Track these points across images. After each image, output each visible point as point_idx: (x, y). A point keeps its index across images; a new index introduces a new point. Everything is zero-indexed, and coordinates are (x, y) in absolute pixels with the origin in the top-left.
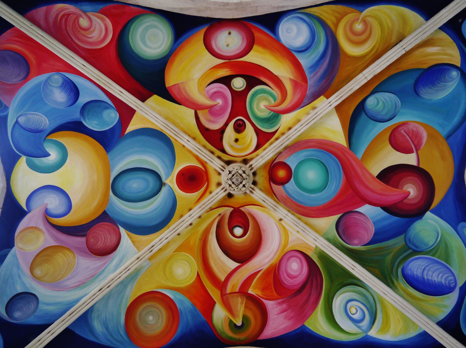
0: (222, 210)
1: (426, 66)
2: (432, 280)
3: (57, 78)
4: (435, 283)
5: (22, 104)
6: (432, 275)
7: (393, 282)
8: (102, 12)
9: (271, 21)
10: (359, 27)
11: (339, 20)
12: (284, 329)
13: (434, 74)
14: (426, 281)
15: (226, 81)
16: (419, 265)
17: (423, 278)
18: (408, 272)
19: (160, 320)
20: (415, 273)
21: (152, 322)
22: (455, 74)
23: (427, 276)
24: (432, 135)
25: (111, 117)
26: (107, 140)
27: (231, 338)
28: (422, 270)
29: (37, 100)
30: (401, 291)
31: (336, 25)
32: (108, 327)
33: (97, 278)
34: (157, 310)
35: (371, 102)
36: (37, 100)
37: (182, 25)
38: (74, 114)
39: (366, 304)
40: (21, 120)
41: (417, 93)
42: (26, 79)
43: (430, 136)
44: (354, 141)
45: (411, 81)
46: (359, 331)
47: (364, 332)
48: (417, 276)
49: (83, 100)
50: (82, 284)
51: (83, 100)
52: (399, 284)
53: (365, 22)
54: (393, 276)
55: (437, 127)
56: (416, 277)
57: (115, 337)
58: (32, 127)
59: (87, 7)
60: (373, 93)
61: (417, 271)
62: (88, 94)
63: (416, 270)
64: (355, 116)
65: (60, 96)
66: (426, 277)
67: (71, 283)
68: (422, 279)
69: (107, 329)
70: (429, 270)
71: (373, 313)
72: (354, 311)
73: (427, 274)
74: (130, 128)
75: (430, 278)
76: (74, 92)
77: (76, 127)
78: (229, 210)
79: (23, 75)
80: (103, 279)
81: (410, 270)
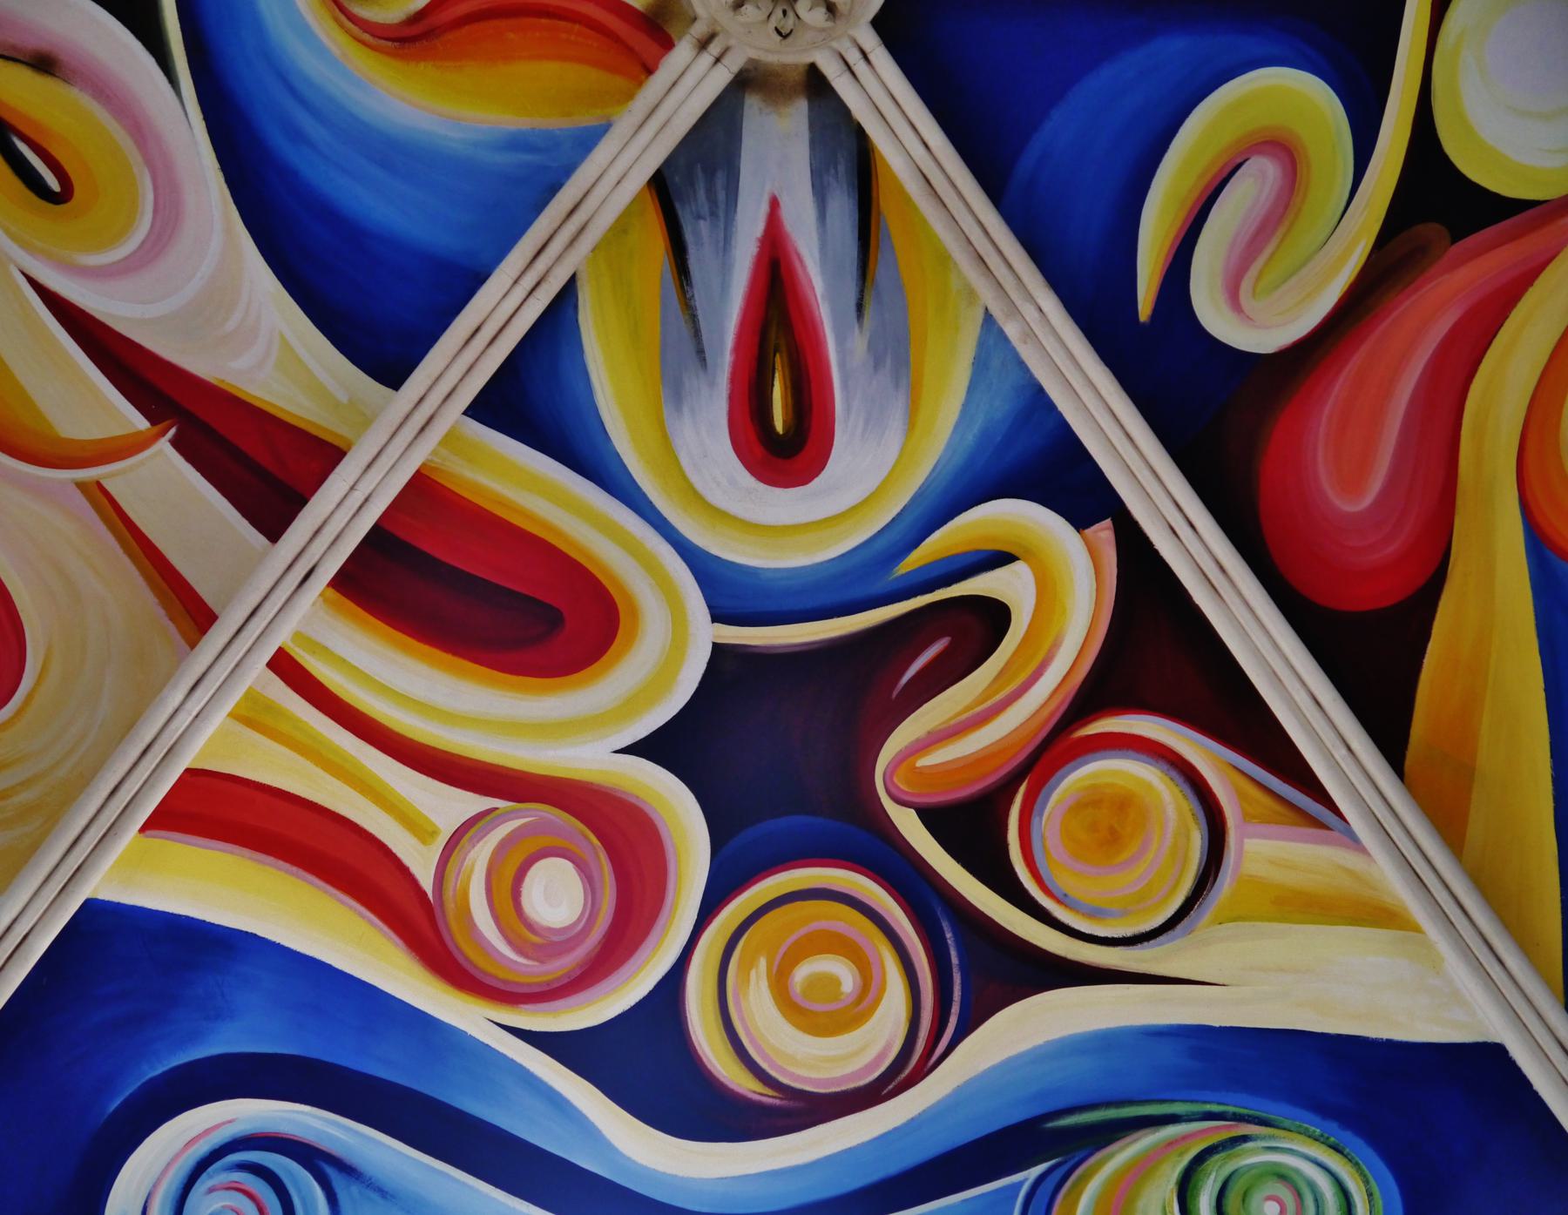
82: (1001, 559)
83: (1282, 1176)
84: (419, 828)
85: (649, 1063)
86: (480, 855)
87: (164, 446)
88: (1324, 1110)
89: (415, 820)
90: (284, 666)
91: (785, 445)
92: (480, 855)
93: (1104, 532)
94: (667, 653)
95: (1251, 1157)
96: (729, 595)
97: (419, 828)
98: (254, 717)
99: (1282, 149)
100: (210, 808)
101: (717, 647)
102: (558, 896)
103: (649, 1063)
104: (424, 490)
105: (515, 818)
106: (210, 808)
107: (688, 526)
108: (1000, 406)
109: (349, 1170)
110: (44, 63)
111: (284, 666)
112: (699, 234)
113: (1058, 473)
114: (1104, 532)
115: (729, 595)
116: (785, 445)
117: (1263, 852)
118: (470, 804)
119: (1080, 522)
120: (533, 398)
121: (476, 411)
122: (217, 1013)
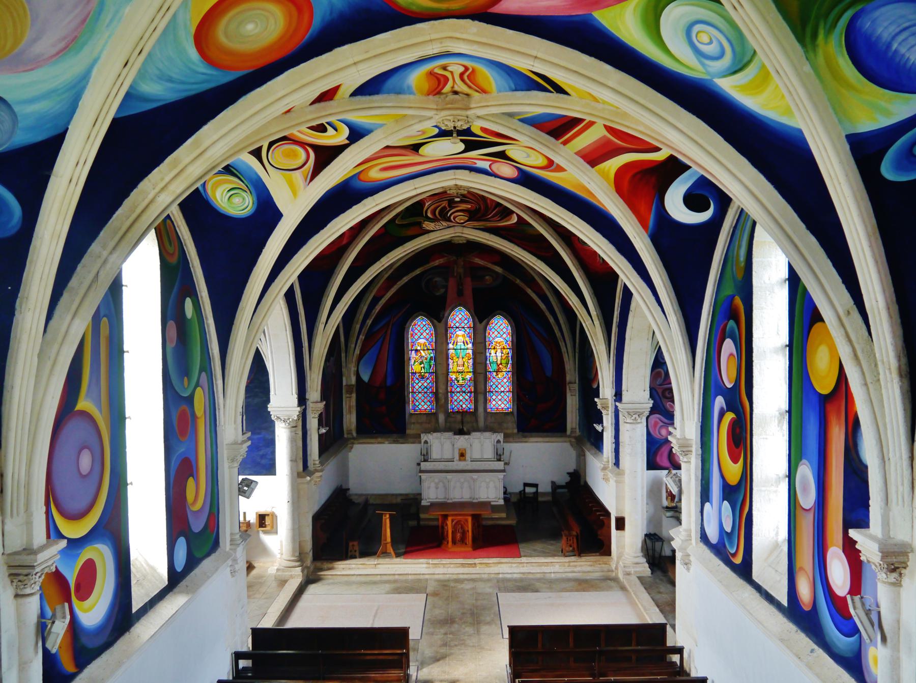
2: (903, 55)
4: (905, 63)
6: (912, 46)
7: (815, 36)
12: (548, 8)
14: (890, 54)
16: (902, 17)
17: (889, 46)
18: (866, 24)
19: (272, 21)
20: (879, 30)
21: (257, 31)
23: (900, 44)
27: (433, 9)
28: (898, 30)
30: (821, 59)
32: (171, 77)
33: (97, 19)
34: (259, 12)
39: (734, 42)
46: (699, 67)
47: (708, 73)
48: (879, 37)
50: (71, 44)
52: (826, 42)
54: (825, 24)
56: (873, 39)
57: (192, 80)
61: (886, 28)
63: (885, 24)
66: (895, 46)
67: (45, 45)
68: (884, 47)
69: (170, 80)
70: (913, 34)
71: (740, 61)
72: (705, 38)
73: (904, 40)
75: (903, 50)
80: (111, 21)
81: (874, 21)
82: (336, 130)
83: (244, 199)
88: (258, 199)
93: (347, 142)
95: (244, 194)
108: (367, 127)
113: (356, 134)
114: (347, 142)
117: (298, 176)
119: (347, 139)
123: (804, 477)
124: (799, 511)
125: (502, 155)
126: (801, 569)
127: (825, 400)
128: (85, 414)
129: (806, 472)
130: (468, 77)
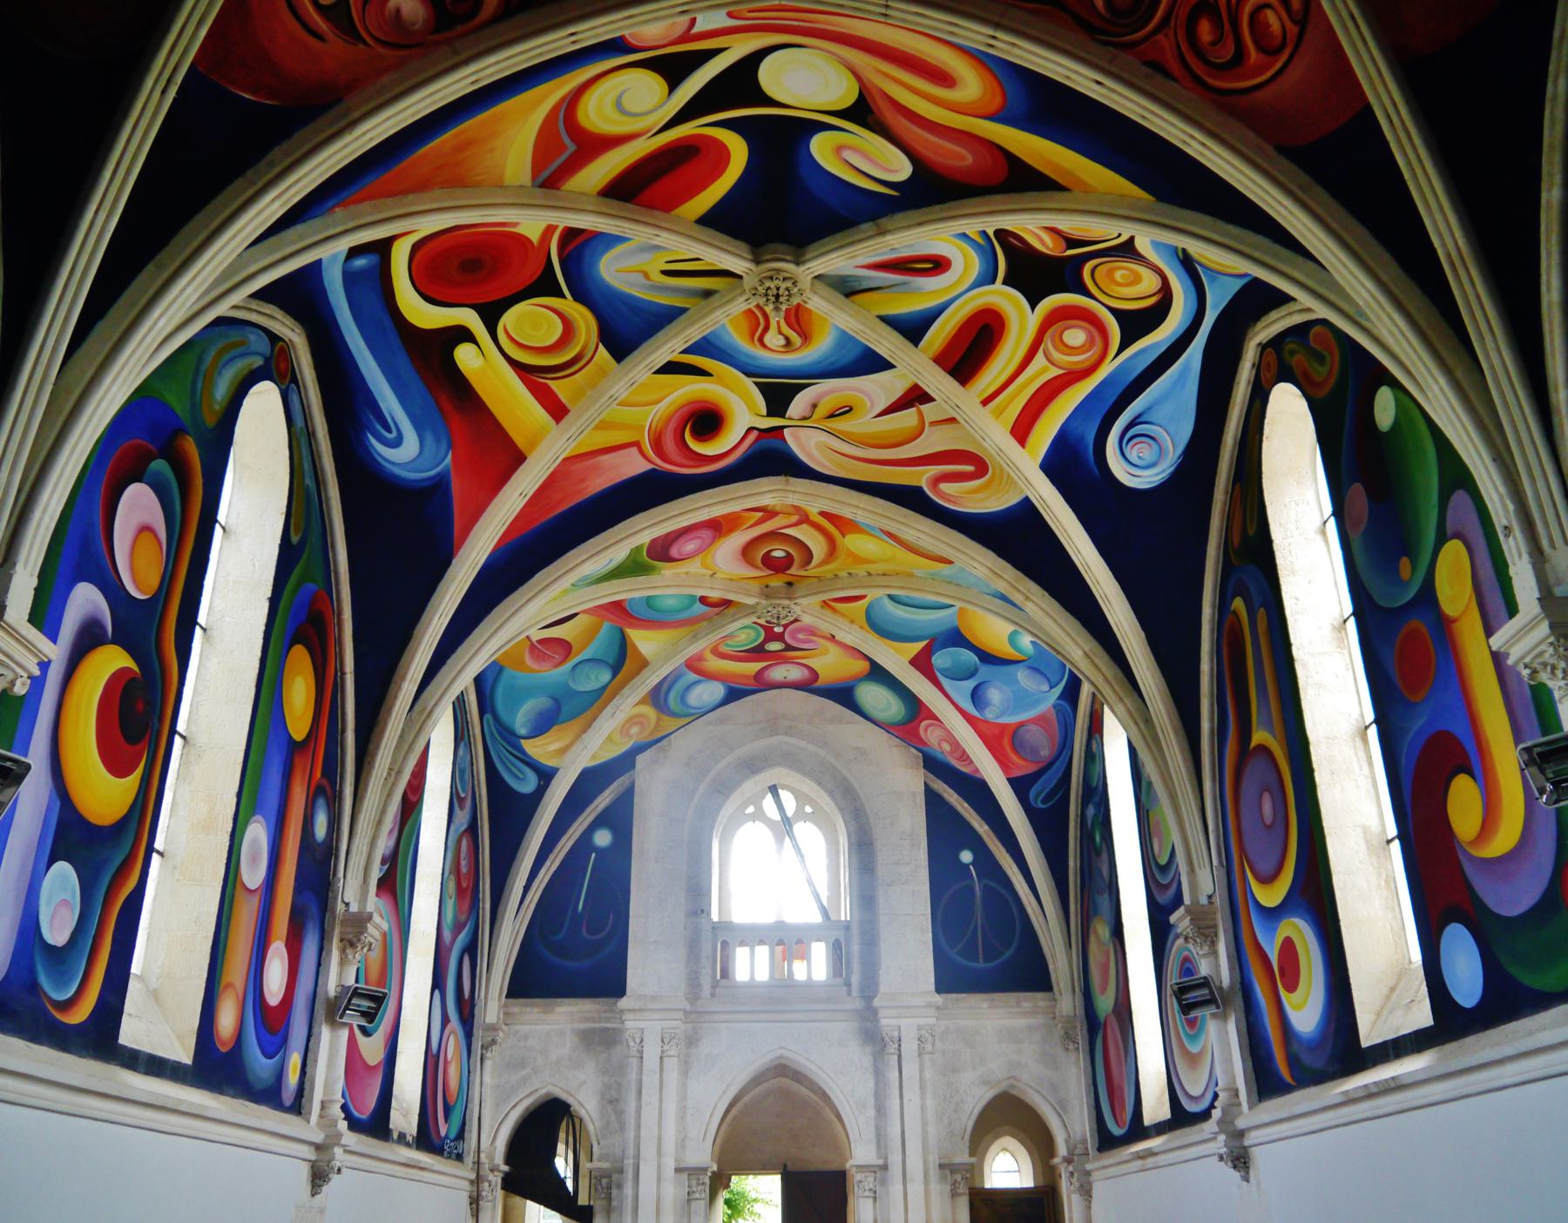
0: (802, 573)
1: (555, 728)
3: (990, 715)
5: (1036, 703)
8: (925, 744)
9: (734, 694)
10: (635, 730)
11: (657, 725)
13: (544, 724)
15: (789, 648)
22: (523, 732)
24: (520, 664)
25: (940, 660)
26: (956, 638)
29: (1021, 699)
31: (659, 719)
35: (605, 676)
36: (1021, 699)
37: (843, 695)
38: (985, 671)
40: (1046, 688)
41: (555, 699)
42: (1021, 724)
43: (522, 662)
44: (618, 635)
45: (566, 709)
49: (971, 684)
51: (971, 684)
53: (628, 735)
55: (518, 674)
58: (1038, 677)
59: (940, 756)
60: (605, 687)
62: (961, 691)
64: (622, 660)
65: (995, 695)
74: (920, 645)
76: (976, 695)
77: (987, 658)
78: (793, 571)
79: (1022, 730)
84: (1045, 370)
85: (1136, 323)
86: (1056, 355)
87: (923, 407)
89: (1041, 371)
90: (985, 402)
91: (938, 265)
92: (1056, 355)
94: (1006, 299)
96: (989, 277)
97: (1045, 370)
98: (999, 413)
99: (839, 149)
100: (1021, 431)
101: (1005, 282)
102: (1076, 336)
103: (1136, 323)
104: (940, 360)
105: (1047, 343)
106: (1021, 431)
107: (962, 286)
109: (1139, 416)
110: (815, 406)
111: (985, 402)
112: (865, 285)
115: (989, 277)
116: (938, 265)
118: (1040, 353)
120: (913, 329)
121: (916, 344)
122: (1081, 439)
123: (255, 841)
124: (239, 893)
125: (673, 68)
126: (229, 985)
127: (294, 749)
128: (1263, 749)
129: (257, 833)
130: (758, 324)
